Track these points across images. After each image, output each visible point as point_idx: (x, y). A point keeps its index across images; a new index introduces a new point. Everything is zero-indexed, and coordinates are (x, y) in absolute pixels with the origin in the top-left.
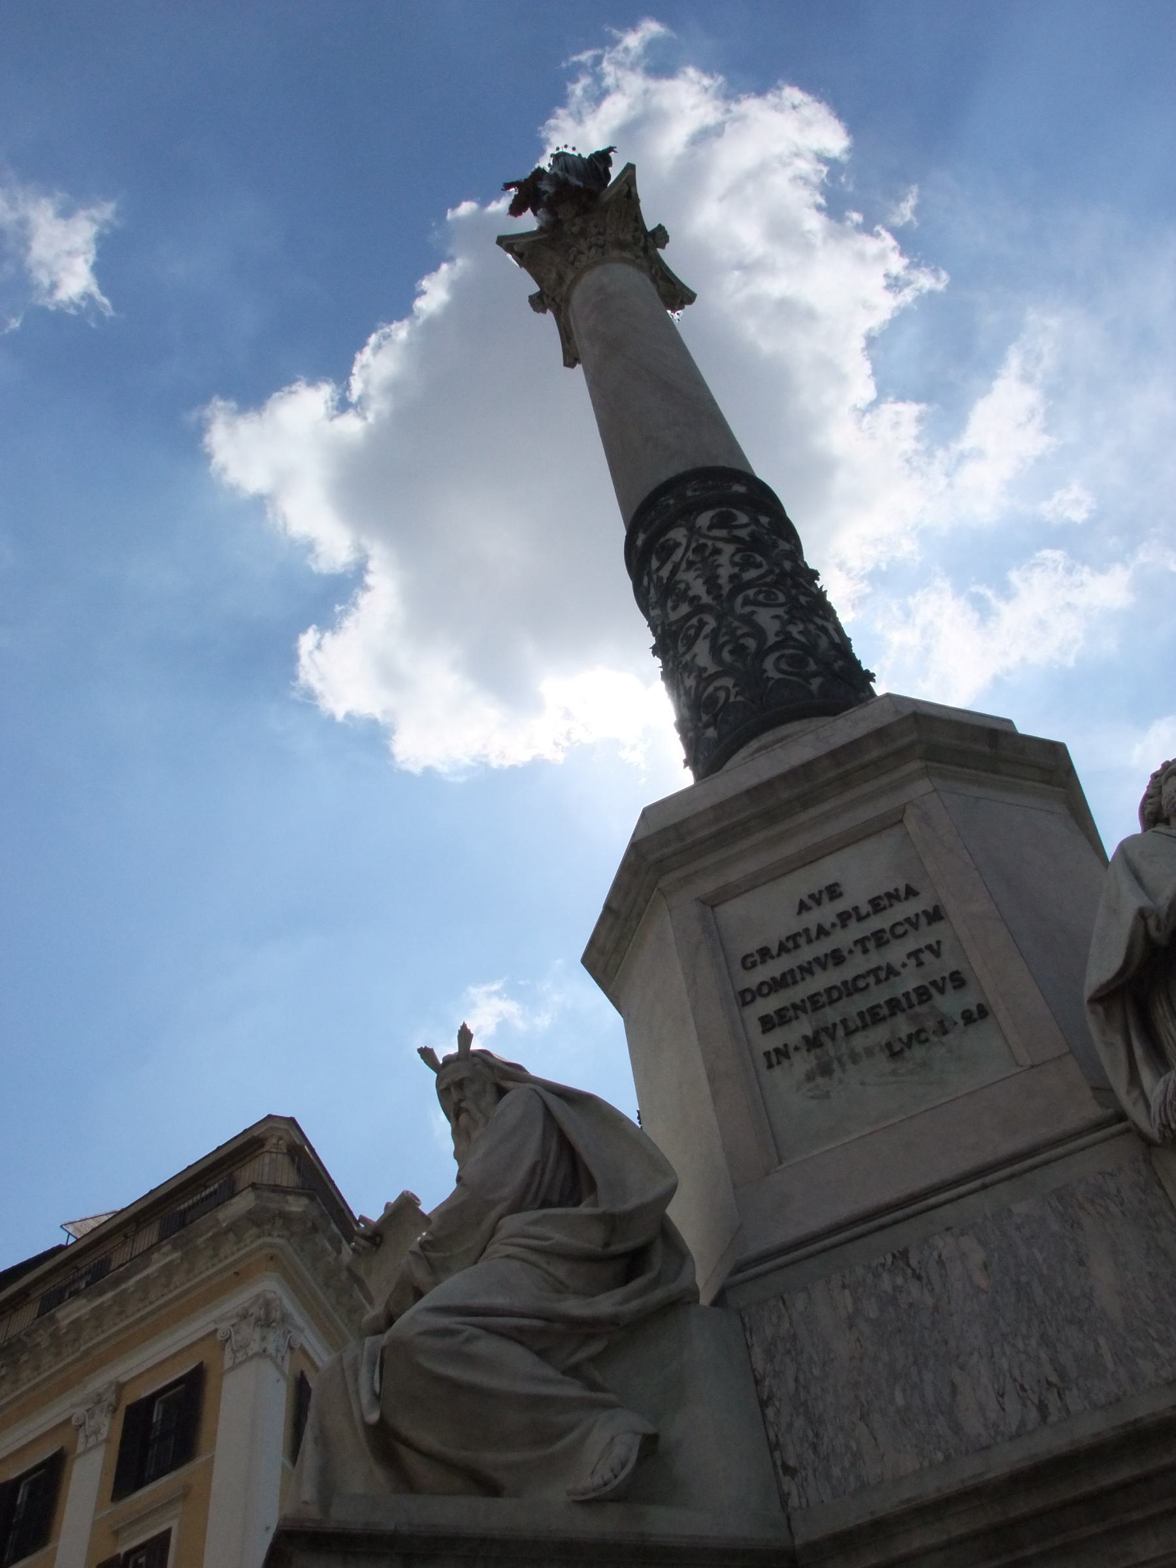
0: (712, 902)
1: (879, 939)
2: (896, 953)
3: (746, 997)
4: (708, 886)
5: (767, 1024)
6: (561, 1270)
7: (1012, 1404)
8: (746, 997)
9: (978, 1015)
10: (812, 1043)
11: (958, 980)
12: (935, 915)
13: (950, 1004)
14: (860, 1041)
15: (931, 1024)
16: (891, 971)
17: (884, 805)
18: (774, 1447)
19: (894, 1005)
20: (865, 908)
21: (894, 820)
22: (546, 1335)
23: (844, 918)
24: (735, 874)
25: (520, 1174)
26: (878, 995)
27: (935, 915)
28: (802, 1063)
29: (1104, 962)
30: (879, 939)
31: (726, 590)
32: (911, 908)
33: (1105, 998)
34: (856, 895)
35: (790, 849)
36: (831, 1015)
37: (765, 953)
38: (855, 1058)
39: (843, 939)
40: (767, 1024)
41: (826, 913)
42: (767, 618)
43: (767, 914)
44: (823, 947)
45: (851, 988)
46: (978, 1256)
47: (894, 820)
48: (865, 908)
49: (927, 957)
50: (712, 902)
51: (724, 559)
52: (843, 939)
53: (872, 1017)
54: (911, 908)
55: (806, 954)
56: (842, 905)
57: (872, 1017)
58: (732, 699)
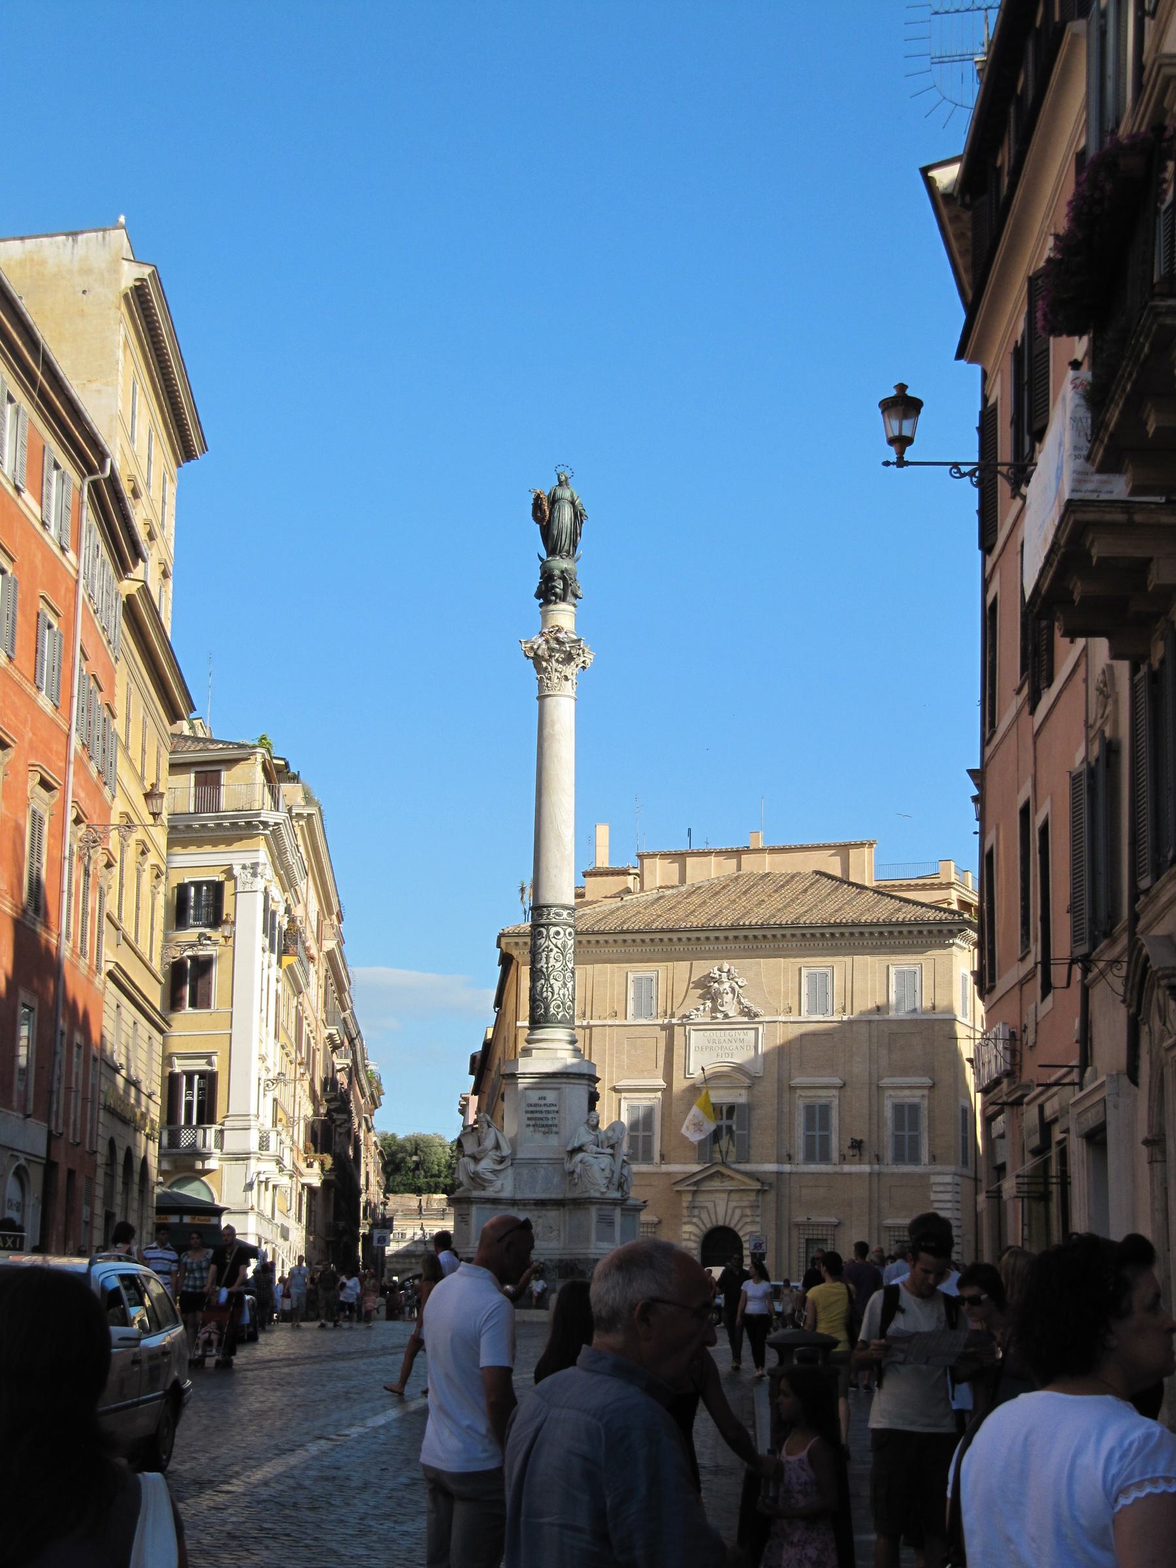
2: (550, 1116)
5: (529, 1119)
8: (527, 1112)
9: (557, 1133)
13: (554, 1129)
22: (494, 1172)
28: (531, 1129)
29: (569, 1148)
30: (548, 1112)
34: (548, 1101)
40: (529, 1119)
41: (542, 1102)
42: (557, 985)
51: (552, 955)
53: (543, 1126)
55: (538, 1109)
57: (543, 1126)
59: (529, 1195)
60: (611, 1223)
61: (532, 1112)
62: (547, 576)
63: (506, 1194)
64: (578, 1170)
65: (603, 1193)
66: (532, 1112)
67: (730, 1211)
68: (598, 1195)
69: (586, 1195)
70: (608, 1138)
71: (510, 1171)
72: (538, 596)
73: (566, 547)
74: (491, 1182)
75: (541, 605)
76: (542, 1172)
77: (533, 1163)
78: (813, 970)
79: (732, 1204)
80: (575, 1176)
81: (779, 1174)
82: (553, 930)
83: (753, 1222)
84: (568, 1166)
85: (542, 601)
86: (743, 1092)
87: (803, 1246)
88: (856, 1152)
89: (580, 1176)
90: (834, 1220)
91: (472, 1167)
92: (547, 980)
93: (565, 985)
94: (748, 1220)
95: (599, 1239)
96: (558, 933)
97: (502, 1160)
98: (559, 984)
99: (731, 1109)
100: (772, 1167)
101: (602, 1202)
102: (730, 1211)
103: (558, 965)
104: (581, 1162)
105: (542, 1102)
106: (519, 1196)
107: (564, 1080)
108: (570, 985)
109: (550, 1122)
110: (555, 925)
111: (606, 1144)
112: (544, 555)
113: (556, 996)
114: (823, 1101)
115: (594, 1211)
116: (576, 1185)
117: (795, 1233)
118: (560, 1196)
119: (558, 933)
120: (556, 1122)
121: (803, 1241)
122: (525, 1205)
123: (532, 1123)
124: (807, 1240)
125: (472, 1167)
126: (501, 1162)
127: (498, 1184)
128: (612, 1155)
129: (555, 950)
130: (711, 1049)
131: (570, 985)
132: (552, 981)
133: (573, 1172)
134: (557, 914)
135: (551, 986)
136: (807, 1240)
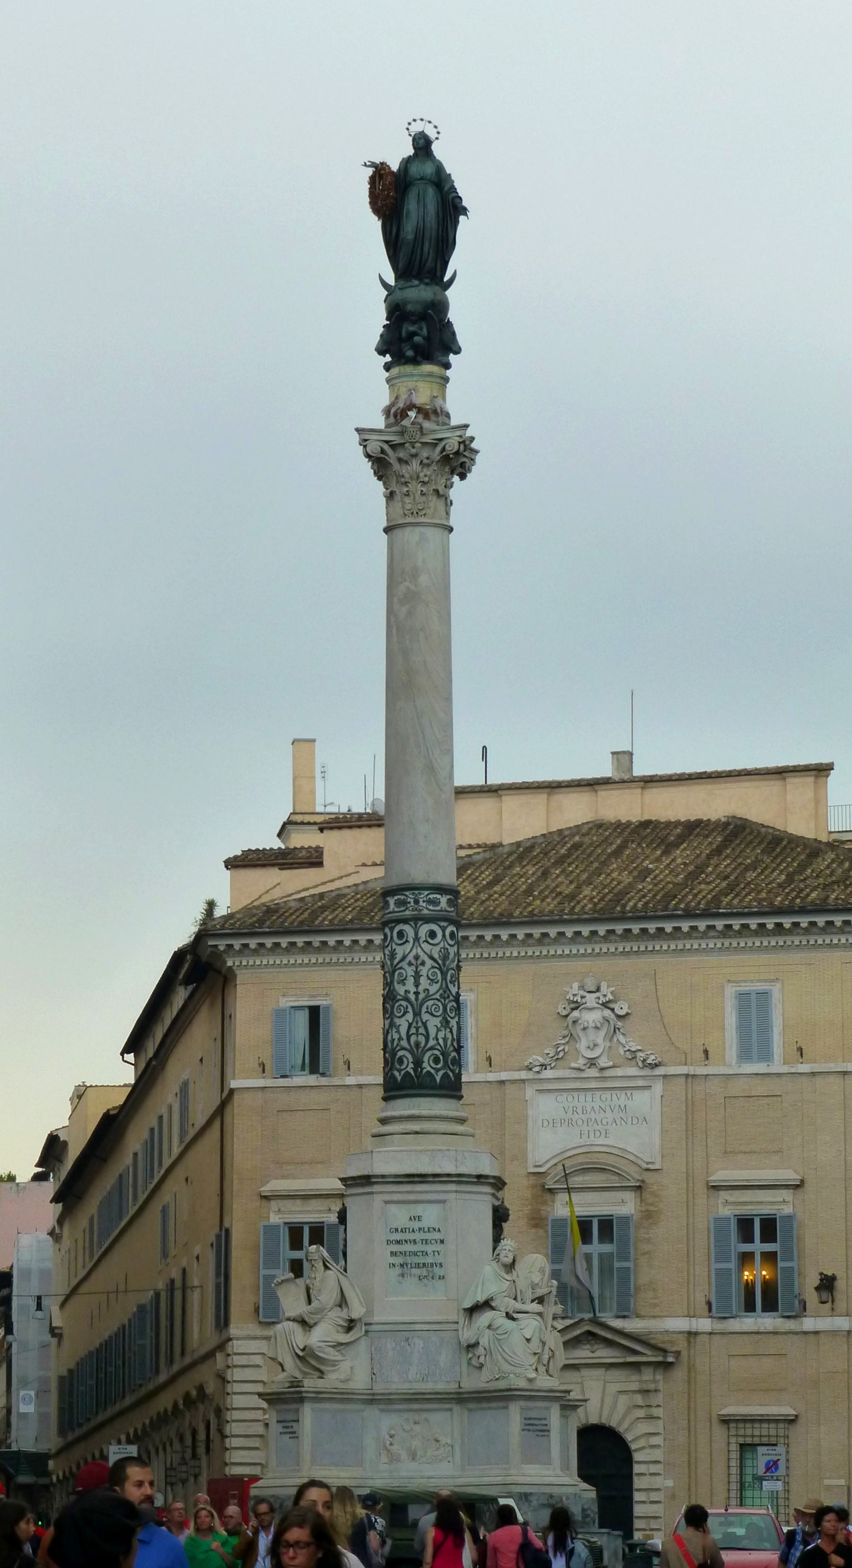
0: (386, 1202)
1: (426, 1242)
2: (429, 1248)
3: (389, 1242)
4: (387, 1197)
5: (393, 1254)
6: (339, 1329)
7: (418, 1376)
8: (389, 1242)
10: (402, 1266)
11: (441, 1265)
12: (442, 1242)
13: (438, 1271)
14: (414, 1271)
15: (431, 1275)
16: (426, 1253)
17: (441, 1197)
18: (372, 1368)
19: (424, 1264)
20: (426, 1230)
21: (443, 1202)
23: (420, 1229)
24: (396, 1197)
25: (333, 1301)
26: (421, 1260)
27: (442, 1242)
28: (398, 1270)
29: (468, 1304)
30: (426, 1242)
31: (422, 996)
32: (437, 1236)
33: (465, 1310)
34: (426, 1223)
35: (412, 1197)
36: (409, 1260)
37: (397, 1230)
38: (411, 1275)
39: (418, 1236)
40: (393, 1254)
41: (416, 1225)
42: (433, 1023)
43: (400, 1216)
44: (411, 1236)
45: (415, 1254)
46: (422, 1345)
47: (443, 1202)
48: (426, 1230)
49: (436, 1253)
50: (386, 1202)
52: (418, 1236)
53: (418, 1266)
54: (437, 1236)
56: (421, 1225)
57: (418, 1266)
58: (408, 1069)
59: (396, 1384)
60: (545, 1431)
61: (398, 1242)
62: (397, 313)
63: (360, 1382)
64: (484, 1342)
65: (530, 1380)
66: (398, 1242)
67: (608, 1400)
68: (522, 1384)
69: (502, 1385)
70: (534, 1286)
71: (363, 1345)
72: (381, 352)
73: (430, 264)
74: (334, 1363)
75: (387, 367)
76: (419, 1344)
77: (403, 1331)
78: (745, 988)
79: (613, 1388)
80: (480, 1350)
81: (691, 1335)
82: (424, 929)
83: (650, 1417)
84: (467, 1335)
85: (388, 358)
86: (629, 1196)
87: (735, 1455)
88: (825, 1295)
89: (488, 1352)
90: (787, 1411)
91: (300, 1338)
92: (417, 1014)
93: (446, 1023)
94: (641, 1413)
95: (528, 1458)
96: (432, 934)
97: (351, 1325)
98: (437, 1021)
99: (607, 1225)
100: (680, 1324)
101: (530, 1396)
102: (608, 1400)
103: (433, 989)
104: (489, 1327)
105: (416, 1225)
106: (379, 1388)
107: (453, 1187)
108: (453, 1023)
109: (429, 1260)
110: (427, 920)
111: (529, 1296)
112: (391, 279)
113: (432, 1043)
114: (766, 1210)
115: (515, 1413)
116: (481, 1367)
117: (719, 1432)
118: (452, 1387)
119: (432, 934)
120: (439, 1259)
121: (734, 1447)
122: (390, 1401)
123: (398, 1260)
124: (742, 1446)
125: (300, 1338)
126: (349, 1329)
127: (345, 1366)
128: (540, 1314)
129: (429, 963)
130: (570, 1123)
131: (453, 1023)
132: (425, 1017)
133: (476, 1345)
134: (435, 902)
135: (425, 1025)
136: (741, 1445)
